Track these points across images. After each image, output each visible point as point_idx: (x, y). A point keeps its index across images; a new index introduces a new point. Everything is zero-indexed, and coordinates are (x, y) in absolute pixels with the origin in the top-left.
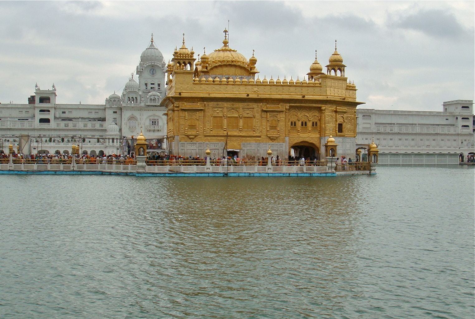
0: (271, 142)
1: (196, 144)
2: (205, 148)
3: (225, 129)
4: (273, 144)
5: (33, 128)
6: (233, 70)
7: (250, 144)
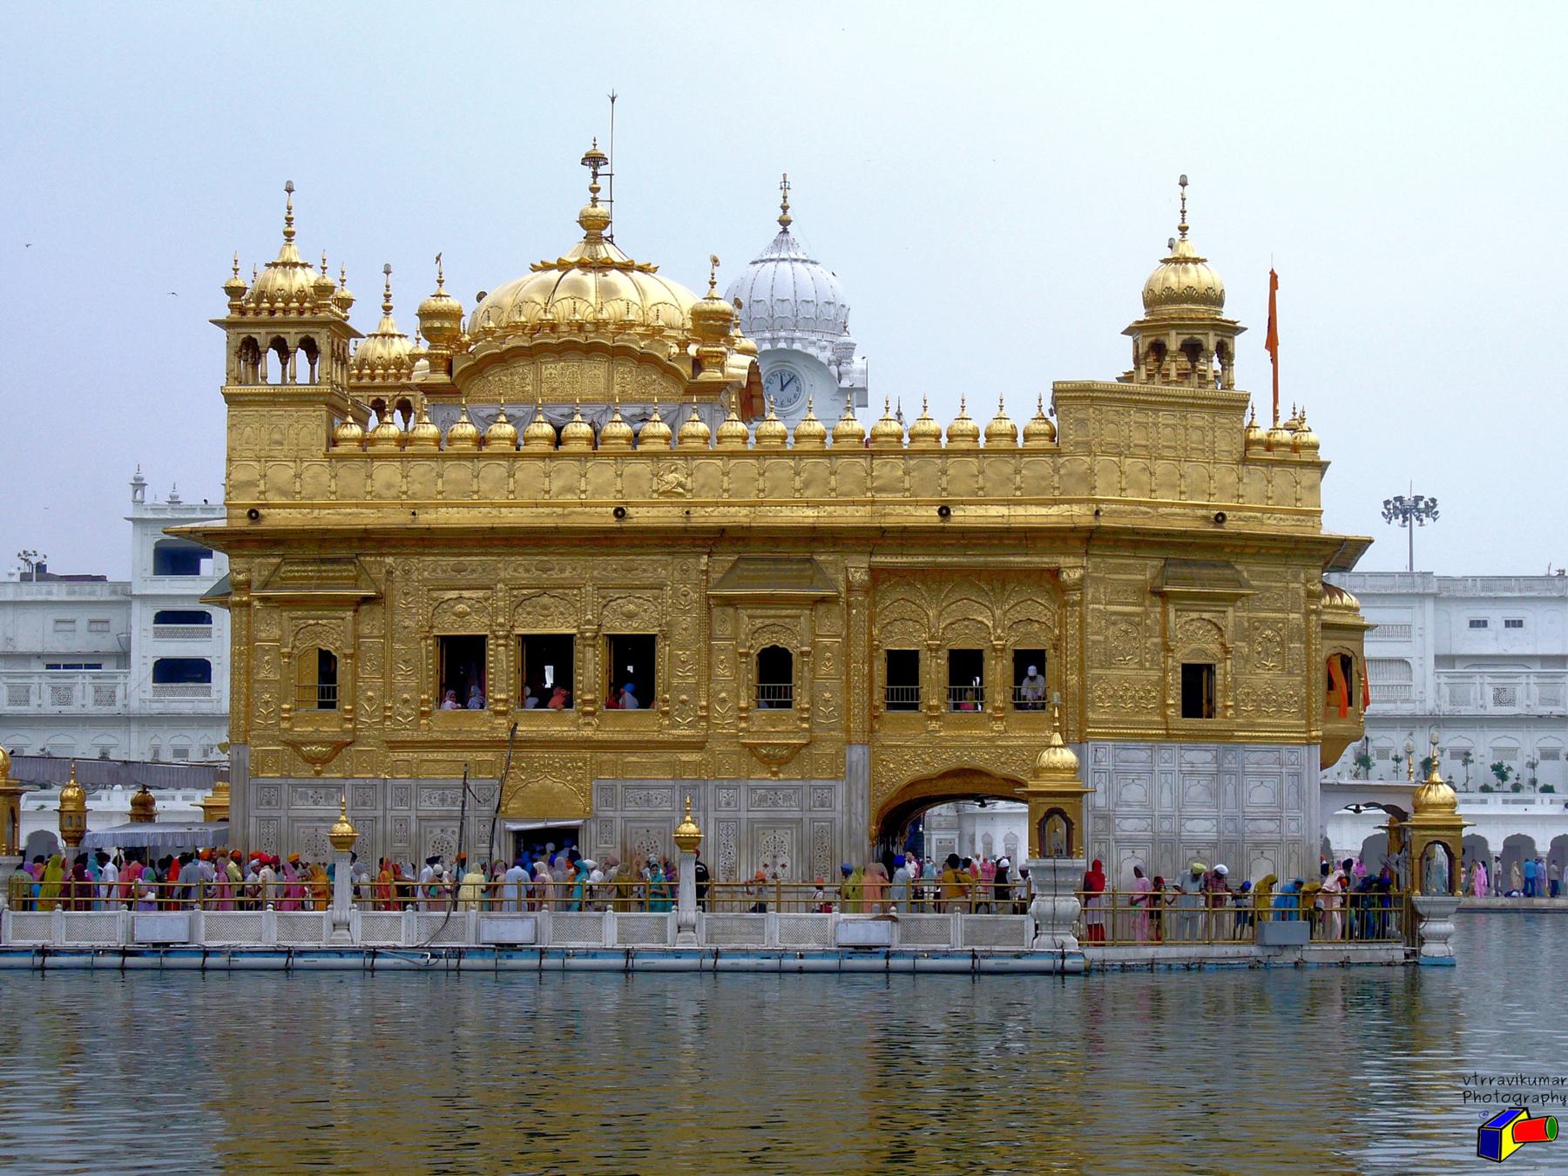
0: (762, 777)
2: (389, 814)
3: (501, 707)
4: (775, 789)
5: (117, 708)
6: (592, 377)
7: (640, 788)
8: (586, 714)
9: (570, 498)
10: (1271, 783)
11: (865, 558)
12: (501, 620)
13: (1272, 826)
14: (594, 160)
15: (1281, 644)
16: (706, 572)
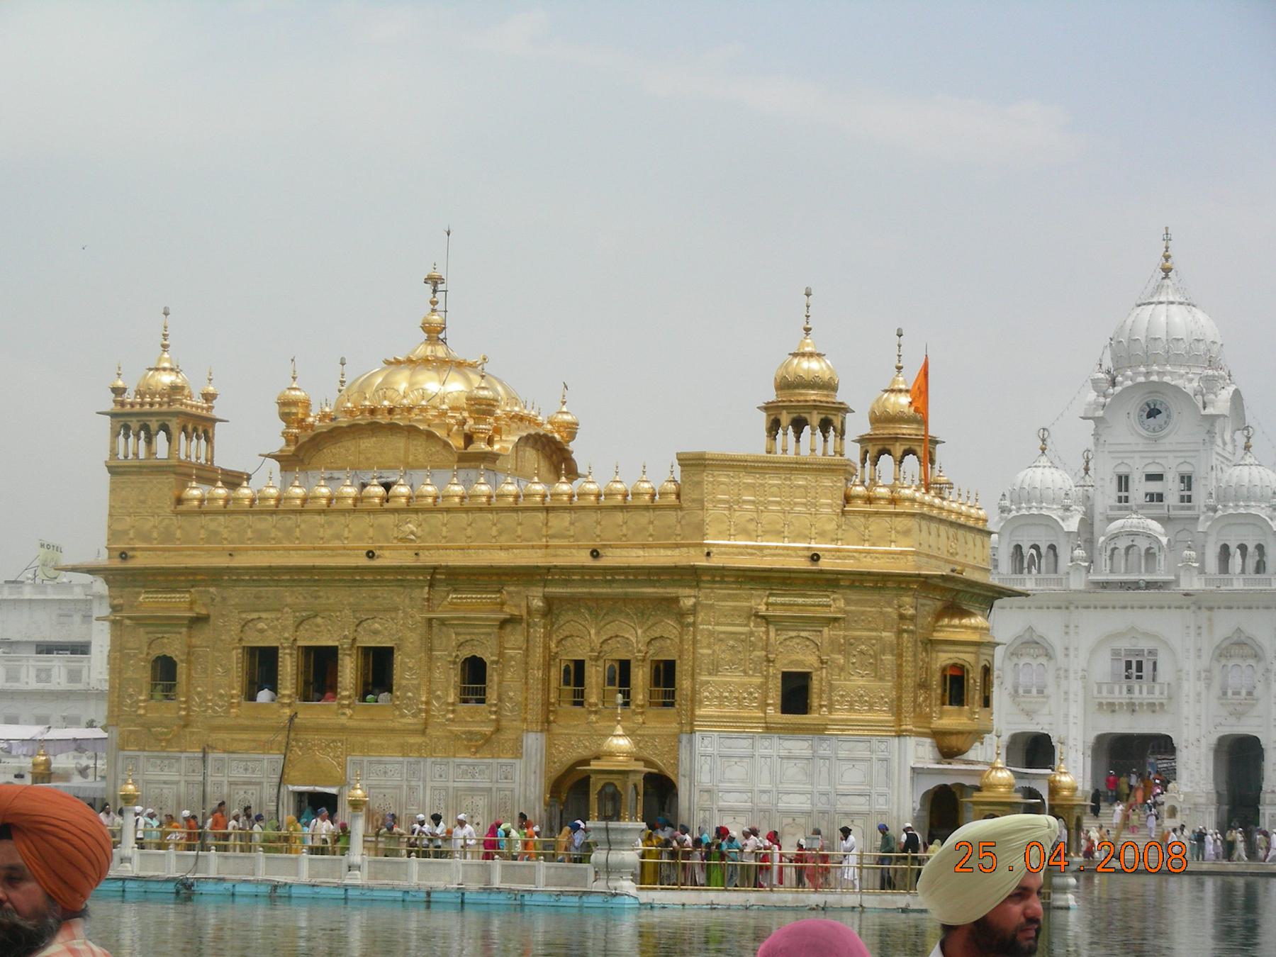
1: (178, 759)
3: (286, 701)
4: (474, 766)
8: (343, 706)
9: (337, 543)
10: (862, 766)
11: (540, 589)
12: (286, 635)
13: (862, 800)
14: (434, 282)
15: (875, 657)
16: (428, 600)
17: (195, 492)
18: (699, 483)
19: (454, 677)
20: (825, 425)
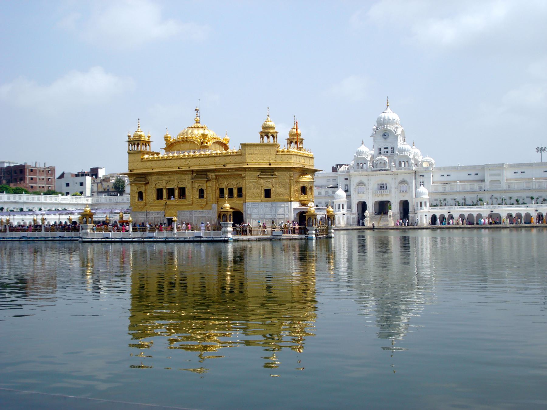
14: (197, 111)
17: (146, 156)
18: (245, 150)
19: (197, 193)
20: (272, 135)
